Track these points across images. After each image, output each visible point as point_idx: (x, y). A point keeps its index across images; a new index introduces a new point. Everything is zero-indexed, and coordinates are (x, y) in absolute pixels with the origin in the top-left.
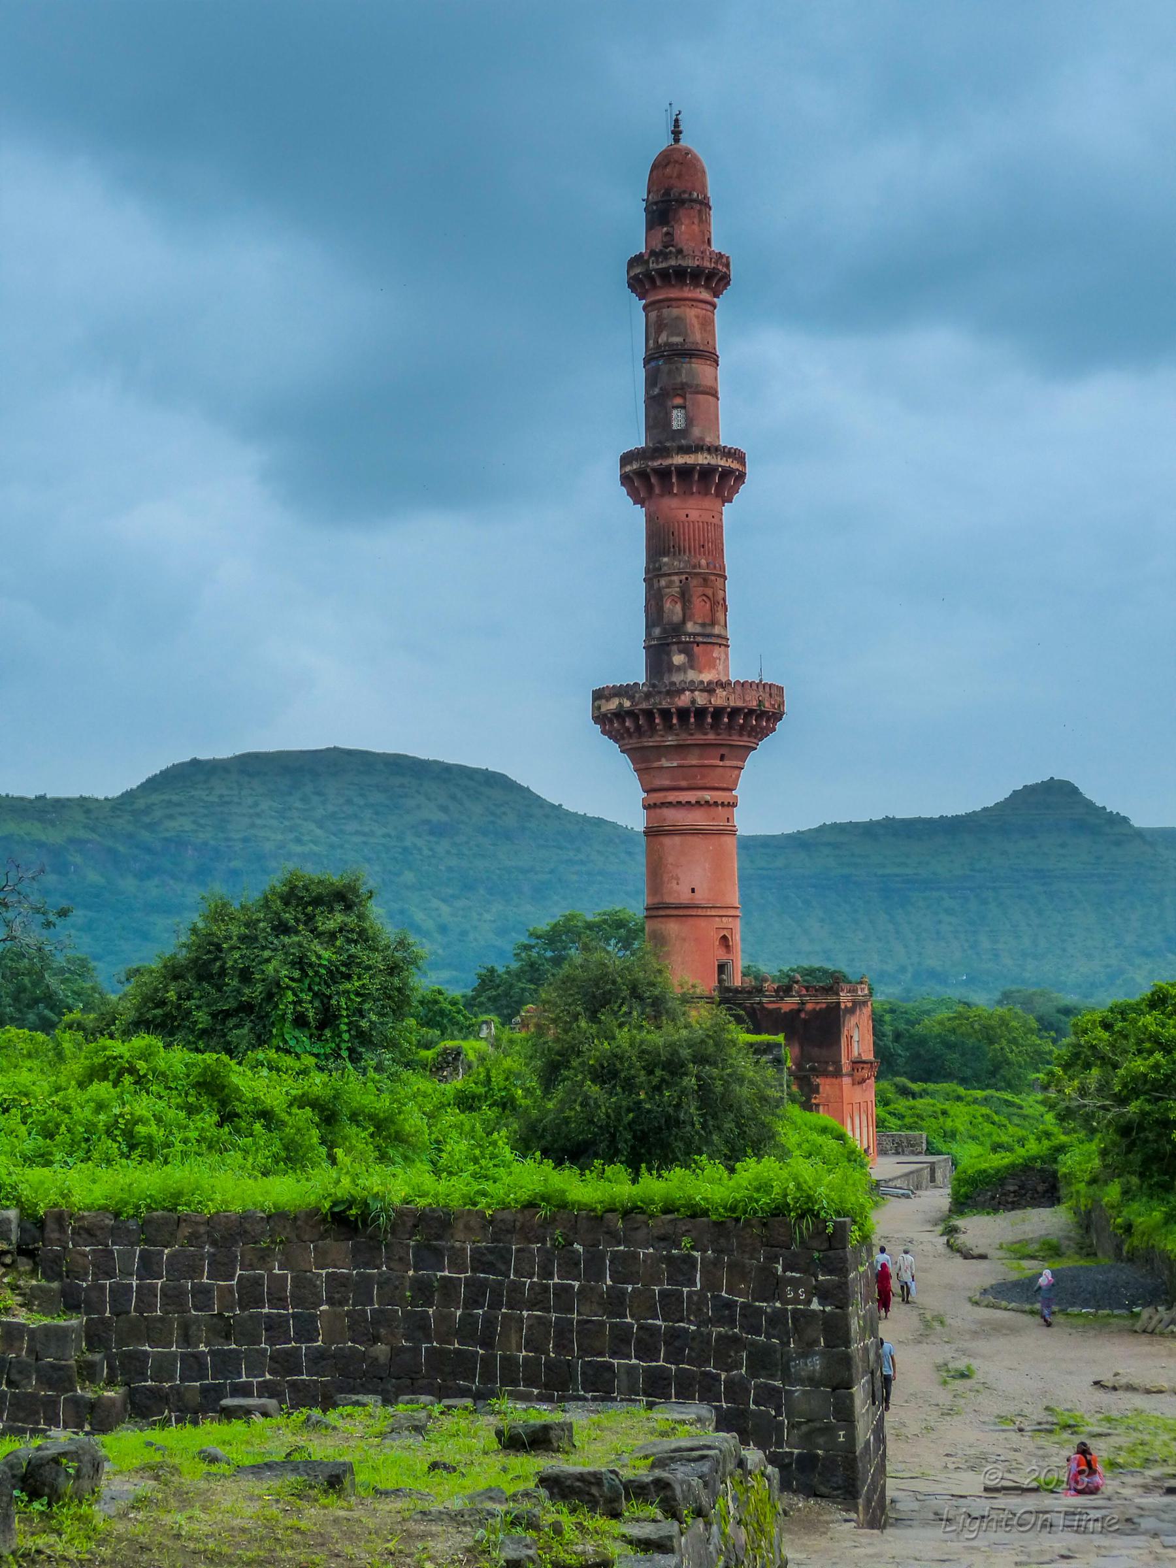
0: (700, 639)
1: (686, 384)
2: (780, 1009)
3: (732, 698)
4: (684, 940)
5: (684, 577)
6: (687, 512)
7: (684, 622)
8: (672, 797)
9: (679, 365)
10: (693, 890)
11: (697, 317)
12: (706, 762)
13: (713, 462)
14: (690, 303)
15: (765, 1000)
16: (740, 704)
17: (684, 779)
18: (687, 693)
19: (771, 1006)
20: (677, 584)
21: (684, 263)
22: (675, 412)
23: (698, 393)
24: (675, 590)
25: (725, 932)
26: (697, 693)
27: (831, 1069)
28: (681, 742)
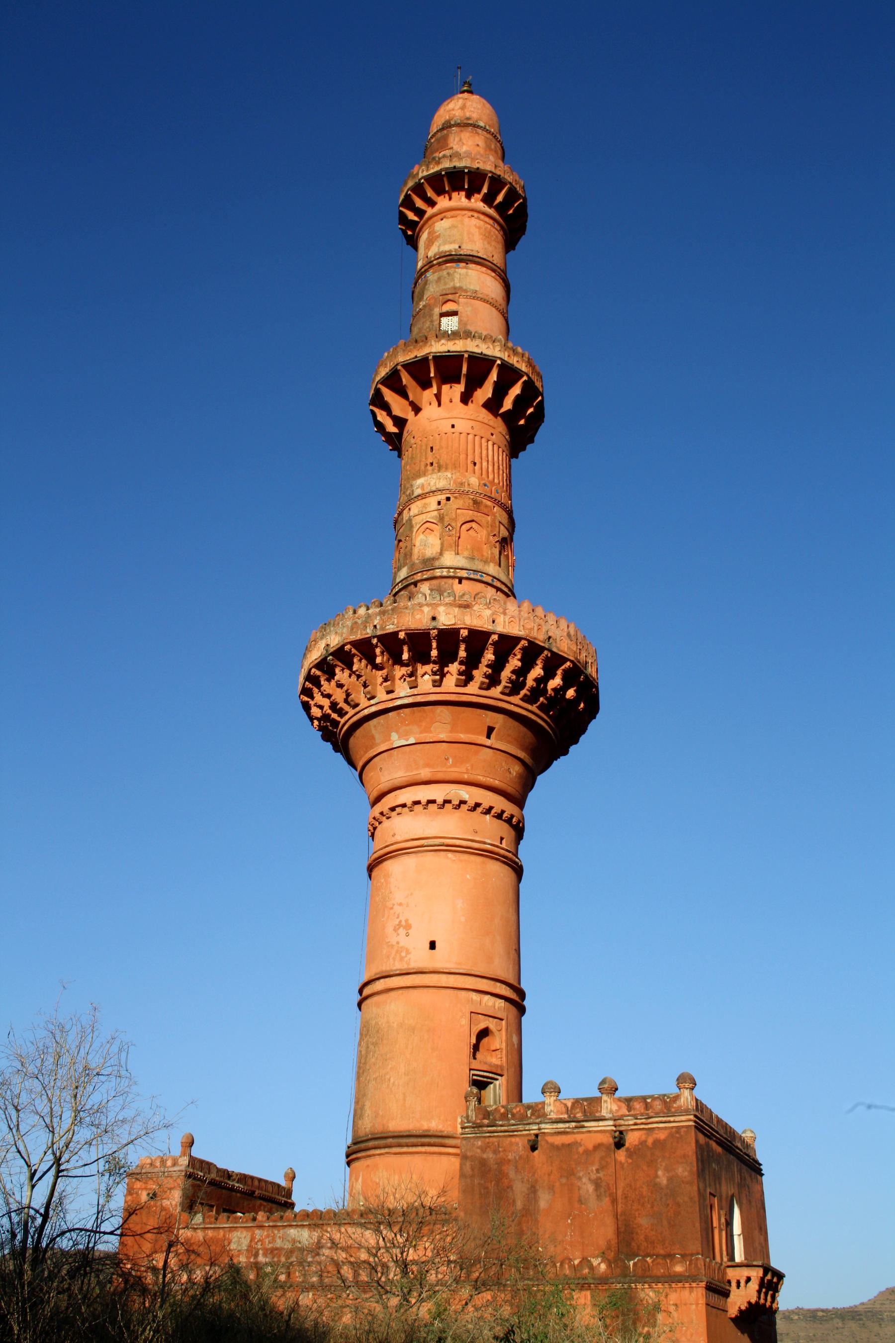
0: (464, 574)
1: (460, 288)
2: (576, 1144)
3: (500, 619)
4: (413, 1029)
5: (444, 497)
6: (453, 422)
7: (441, 554)
8: (406, 796)
9: (451, 271)
10: (433, 945)
11: (479, 228)
12: (463, 737)
13: (489, 352)
14: (470, 213)
15: (547, 1128)
16: (515, 630)
17: (428, 765)
18: (426, 609)
19: (559, 1140)
20: (434, 506)
21: (460, 164)
22: (444, 320)
23: (474, 298)
24: (432, 516)
25: (491, 1024)
26: (441, 609)
27: (679, 1268)
28: (419, 699)
